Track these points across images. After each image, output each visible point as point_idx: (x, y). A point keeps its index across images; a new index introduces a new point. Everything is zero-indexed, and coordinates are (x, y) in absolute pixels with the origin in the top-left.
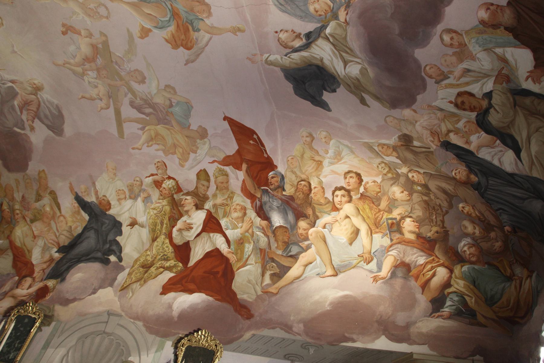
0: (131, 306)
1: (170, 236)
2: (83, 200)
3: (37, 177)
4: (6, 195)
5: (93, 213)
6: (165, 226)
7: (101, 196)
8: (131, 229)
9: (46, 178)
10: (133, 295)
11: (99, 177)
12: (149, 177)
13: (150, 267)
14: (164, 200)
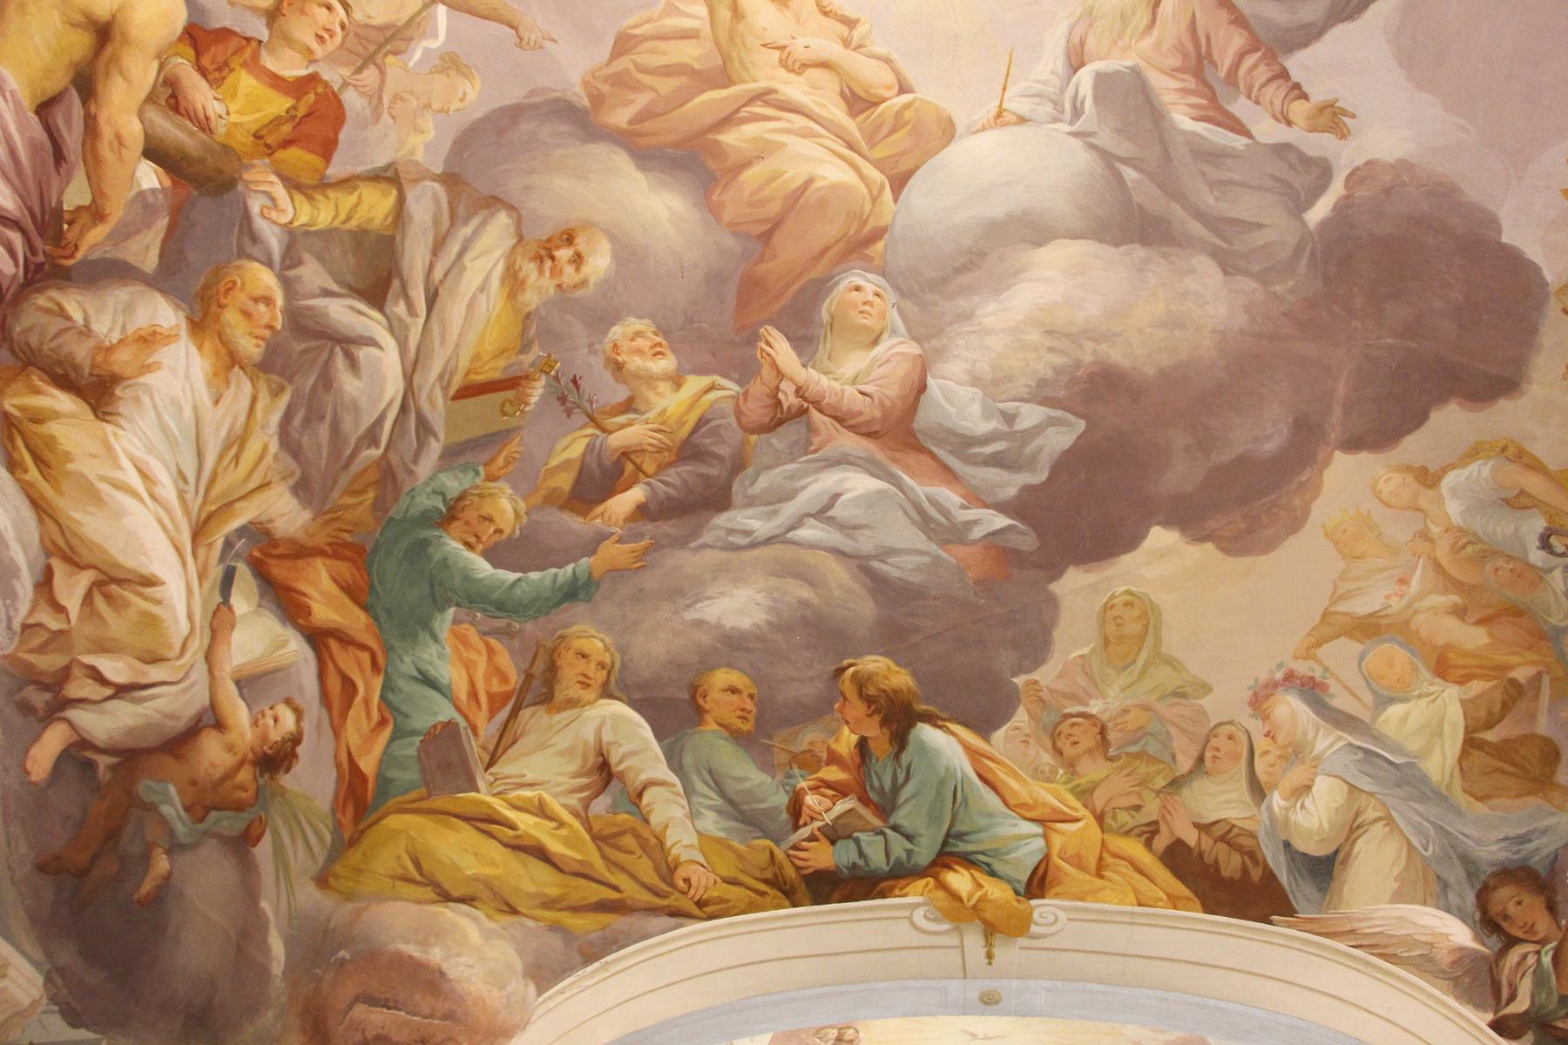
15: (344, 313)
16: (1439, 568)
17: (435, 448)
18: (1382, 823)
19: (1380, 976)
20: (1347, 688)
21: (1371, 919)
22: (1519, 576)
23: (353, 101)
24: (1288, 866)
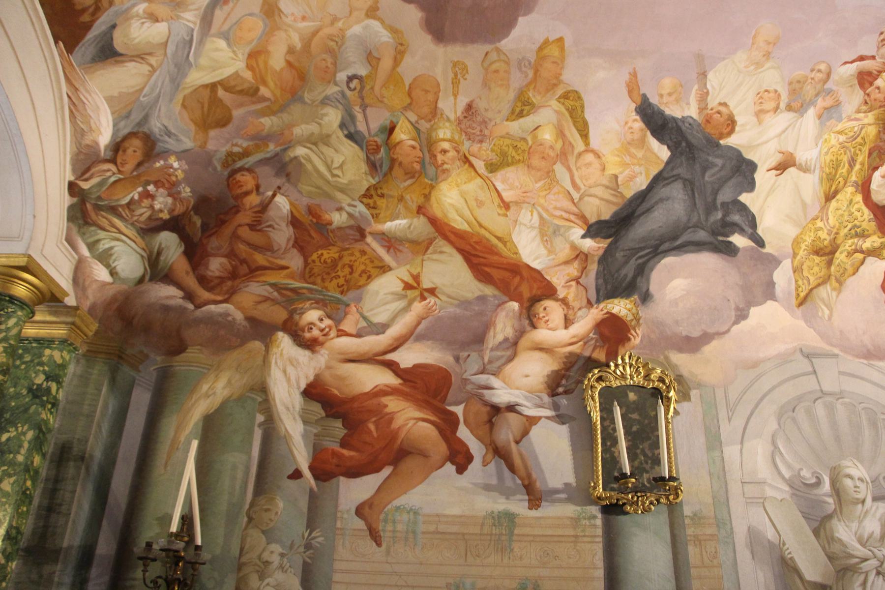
0: (841, 332)
1: (865, 188)
2: (661, 113)
3: (532, 57)
4: (410, 104)
5: (684, 144)
6: (858, 167)
7: (713, 102)
8: (776, 176)
9: (560, 63)
10: (831, 310)
11: (724, 59)
12: (852, 62)
13: (833, 252)
14: (870, 114)
16: (315, 33)
18: (150, 69)
19: (60, 119)
20: (229, 14)
21: (90, 95)
22: (325, 72)
24: (100, 35)
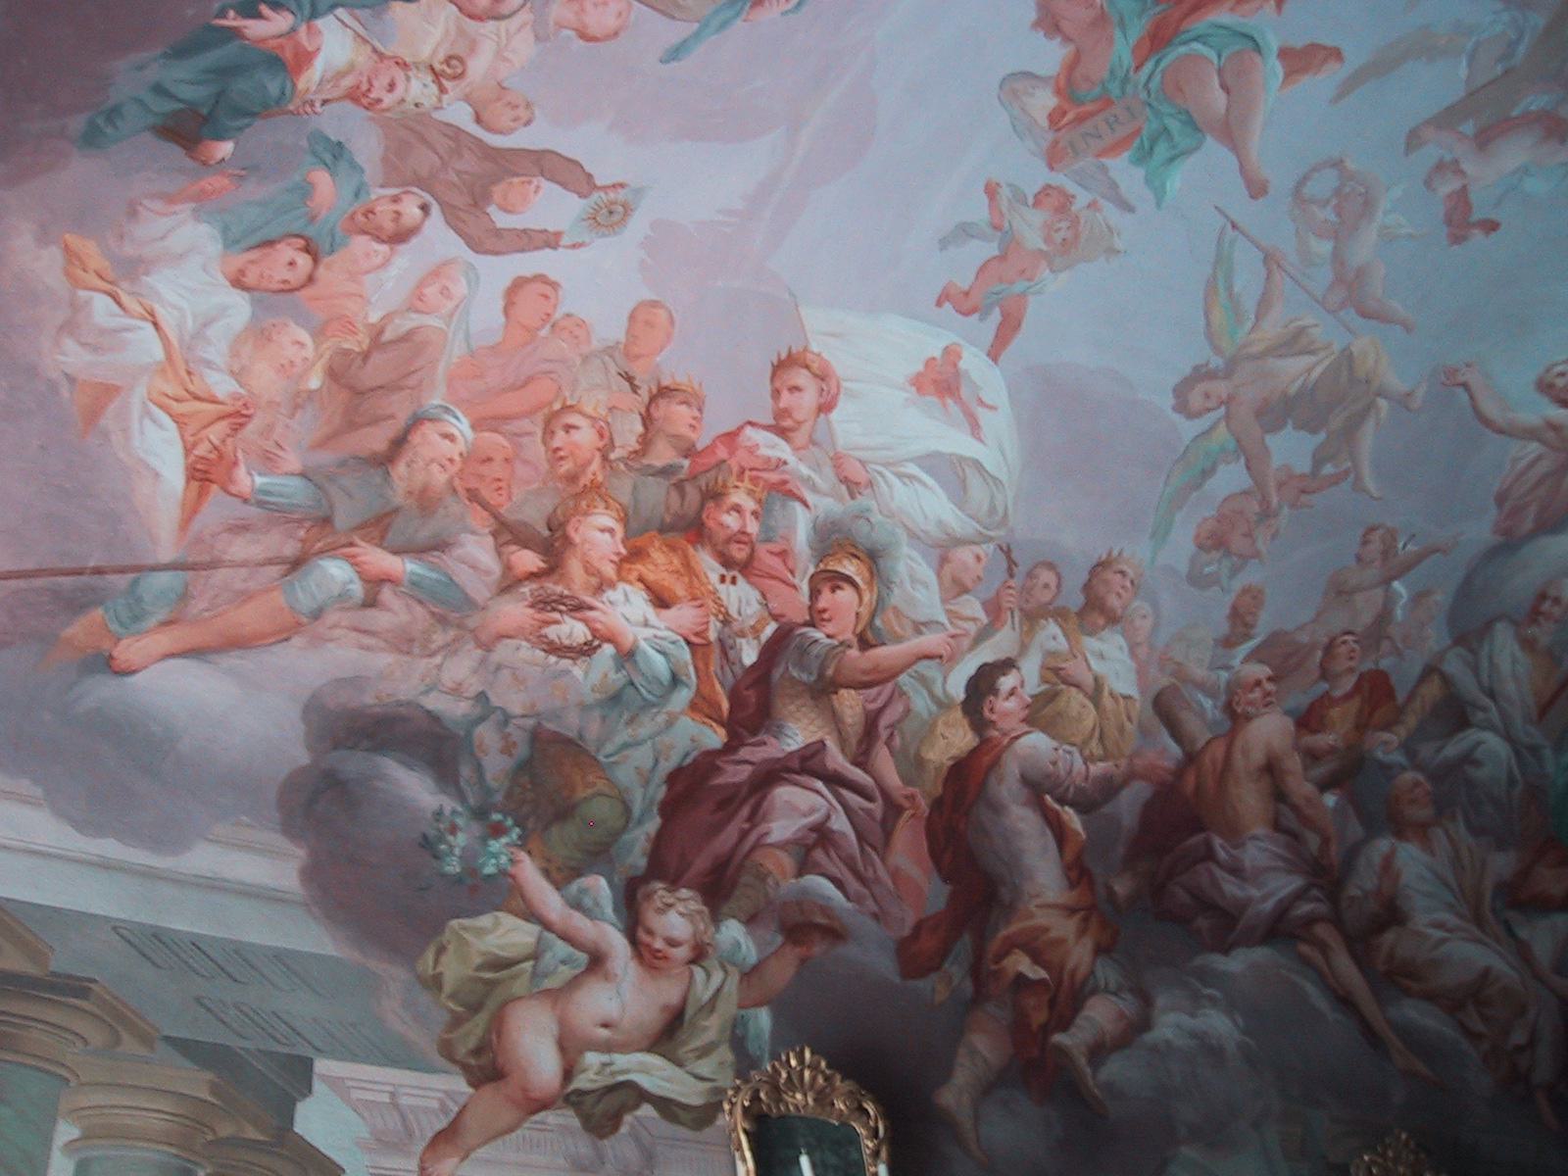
15: (1452, 749)
17: (1548, 753)
23: (1385, 664)
